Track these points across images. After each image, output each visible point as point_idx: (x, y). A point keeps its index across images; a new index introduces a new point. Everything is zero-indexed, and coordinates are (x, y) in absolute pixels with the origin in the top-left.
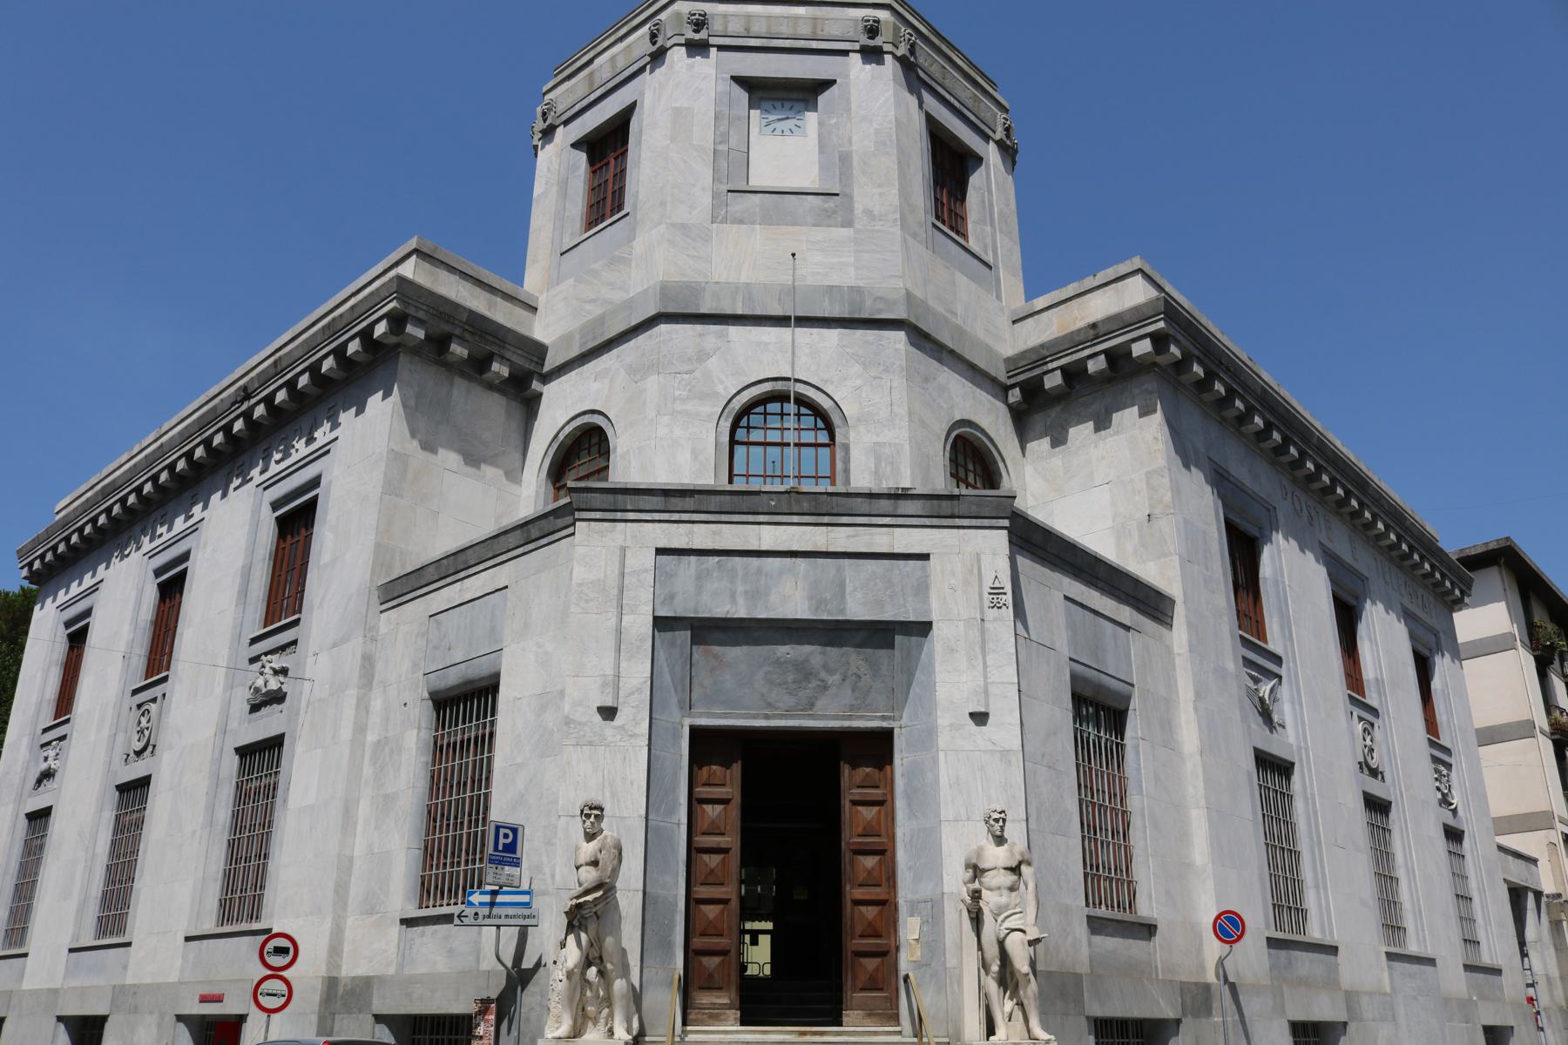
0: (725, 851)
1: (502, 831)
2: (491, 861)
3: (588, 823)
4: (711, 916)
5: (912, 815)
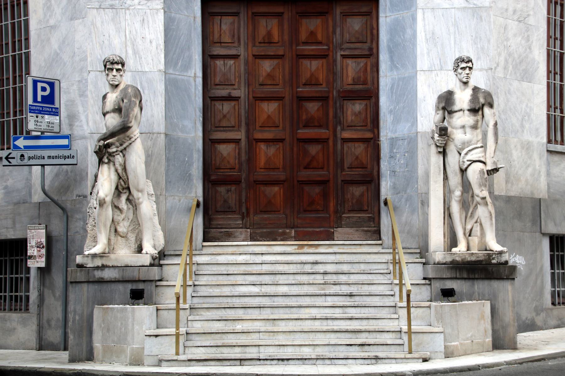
0: (237, 99)
1: (40, 85)
2: (32, 111)
3: (111, 76)
4: (225, 153)
5: (393, 66)
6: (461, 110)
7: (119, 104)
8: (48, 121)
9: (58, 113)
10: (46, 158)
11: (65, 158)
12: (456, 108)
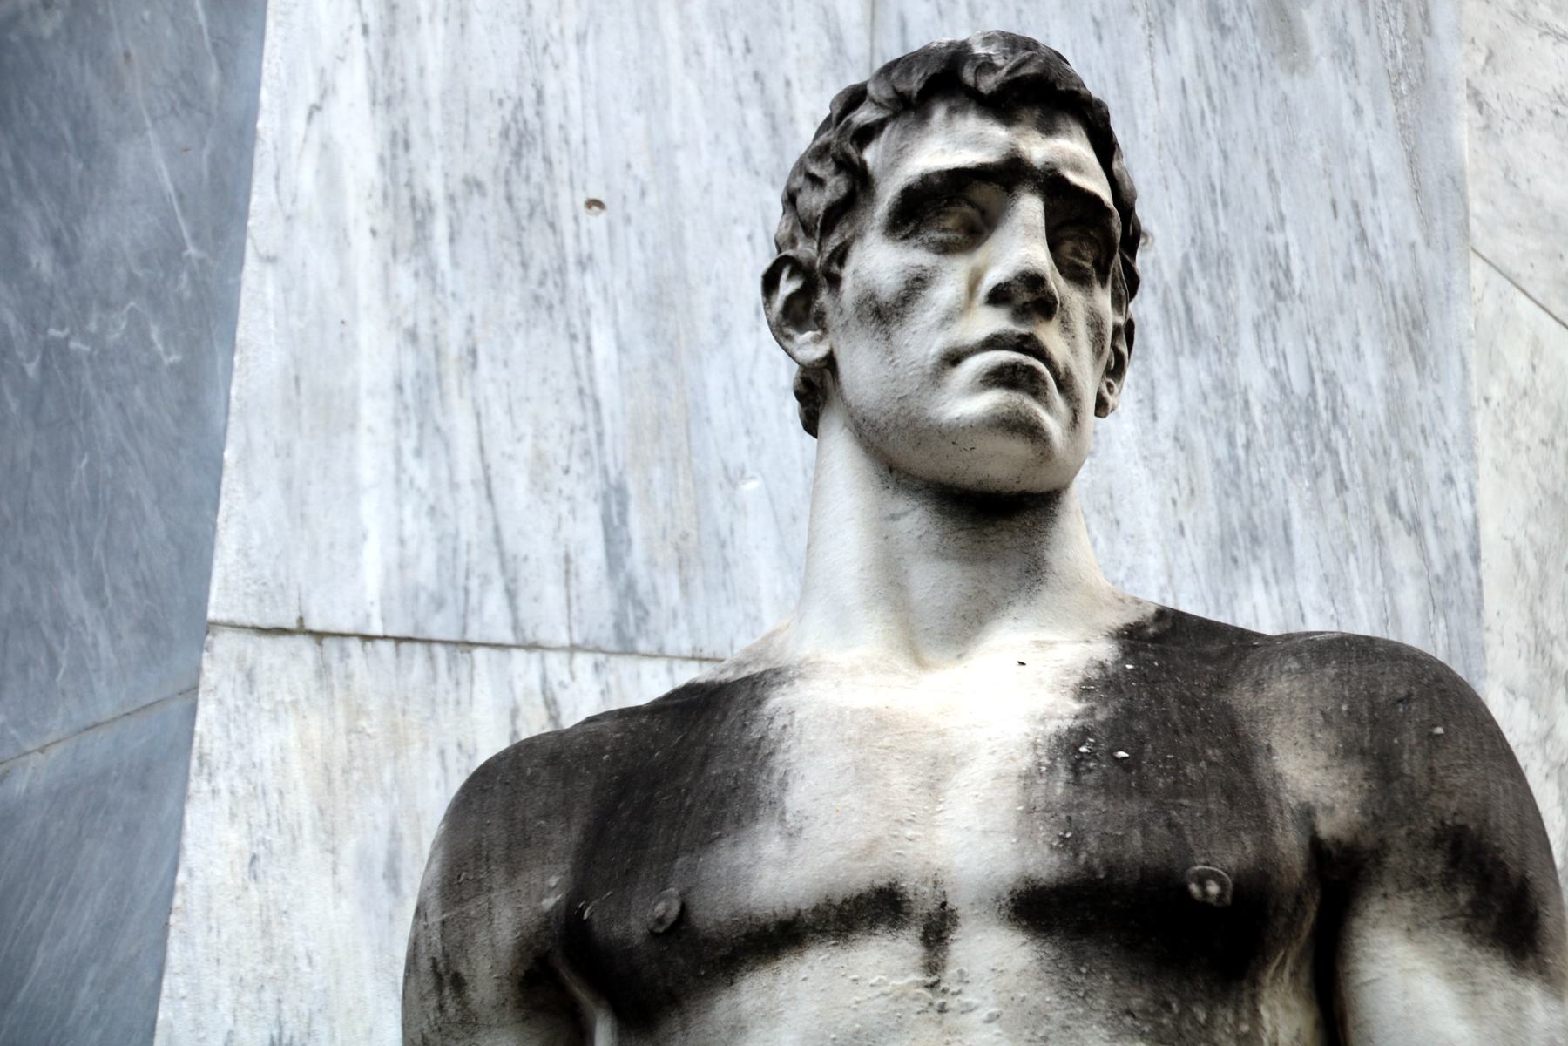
6: (876, 908)
12: (776, 867)
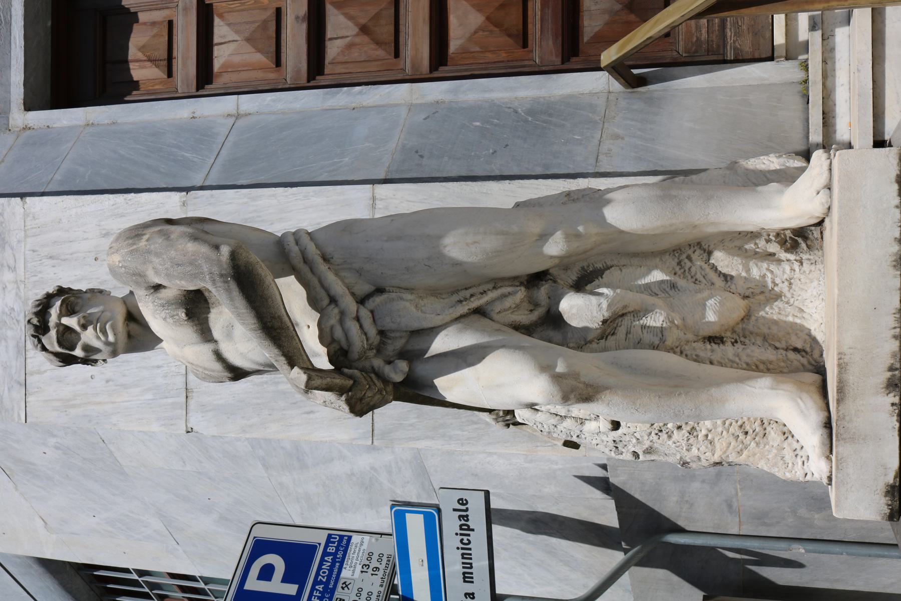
7: (168, 304)
8: (359, 568)
9: (342, 537)
10: (469, 588)
11: (466, 528)
